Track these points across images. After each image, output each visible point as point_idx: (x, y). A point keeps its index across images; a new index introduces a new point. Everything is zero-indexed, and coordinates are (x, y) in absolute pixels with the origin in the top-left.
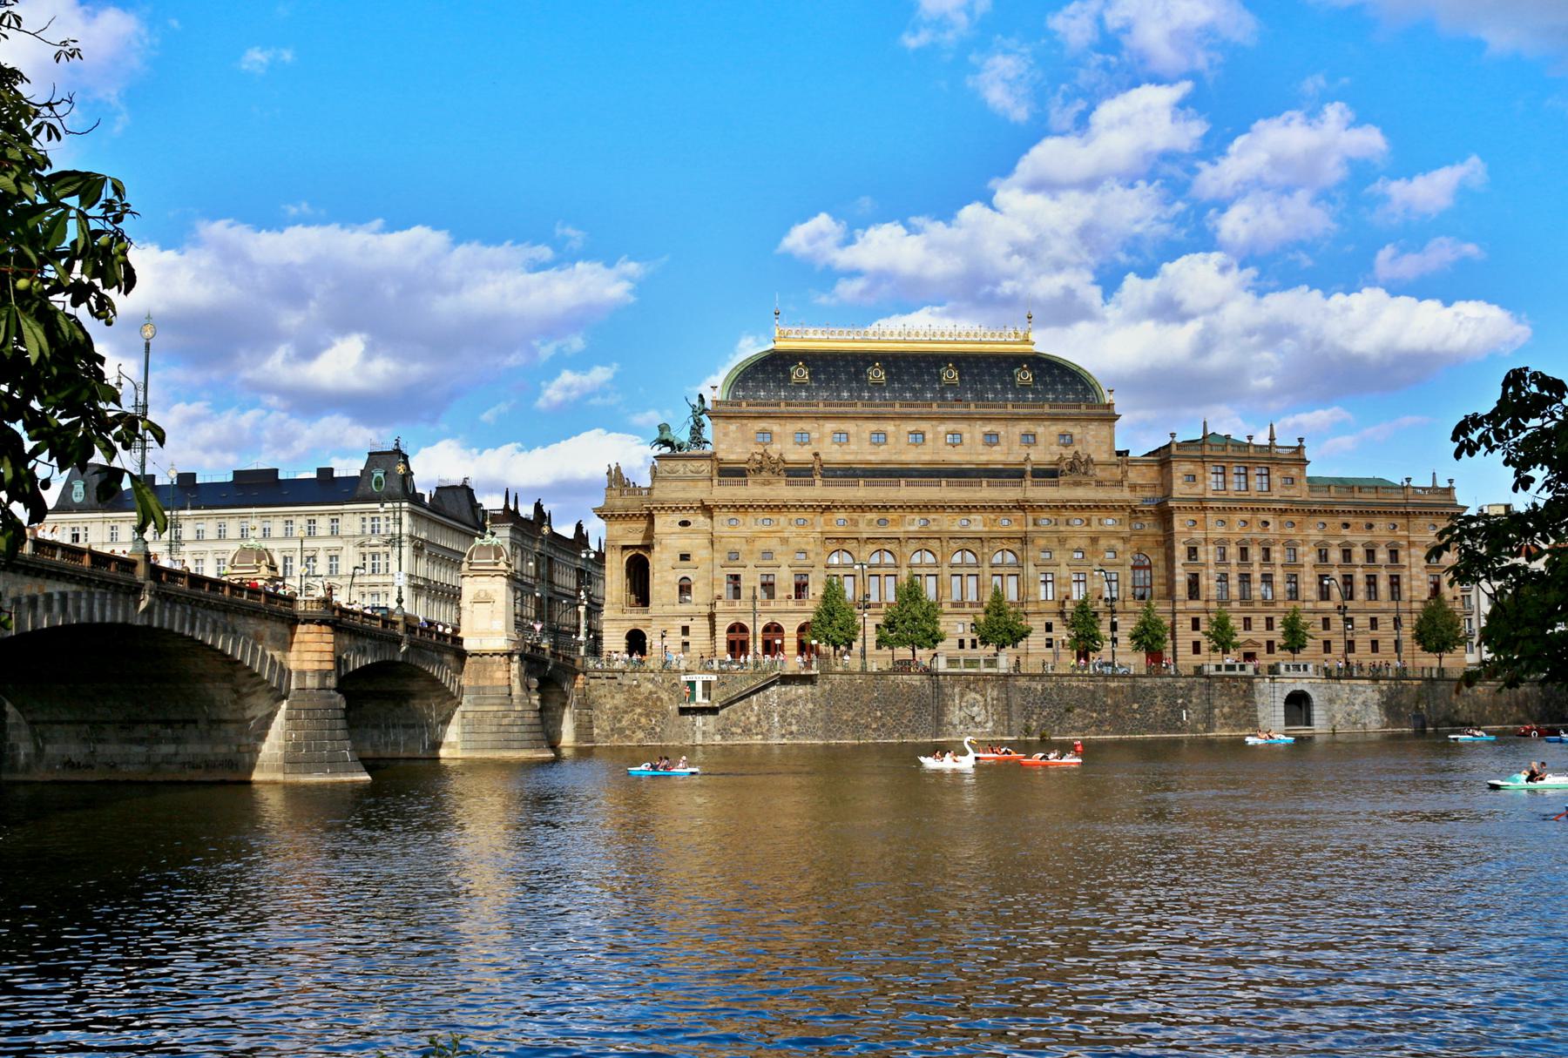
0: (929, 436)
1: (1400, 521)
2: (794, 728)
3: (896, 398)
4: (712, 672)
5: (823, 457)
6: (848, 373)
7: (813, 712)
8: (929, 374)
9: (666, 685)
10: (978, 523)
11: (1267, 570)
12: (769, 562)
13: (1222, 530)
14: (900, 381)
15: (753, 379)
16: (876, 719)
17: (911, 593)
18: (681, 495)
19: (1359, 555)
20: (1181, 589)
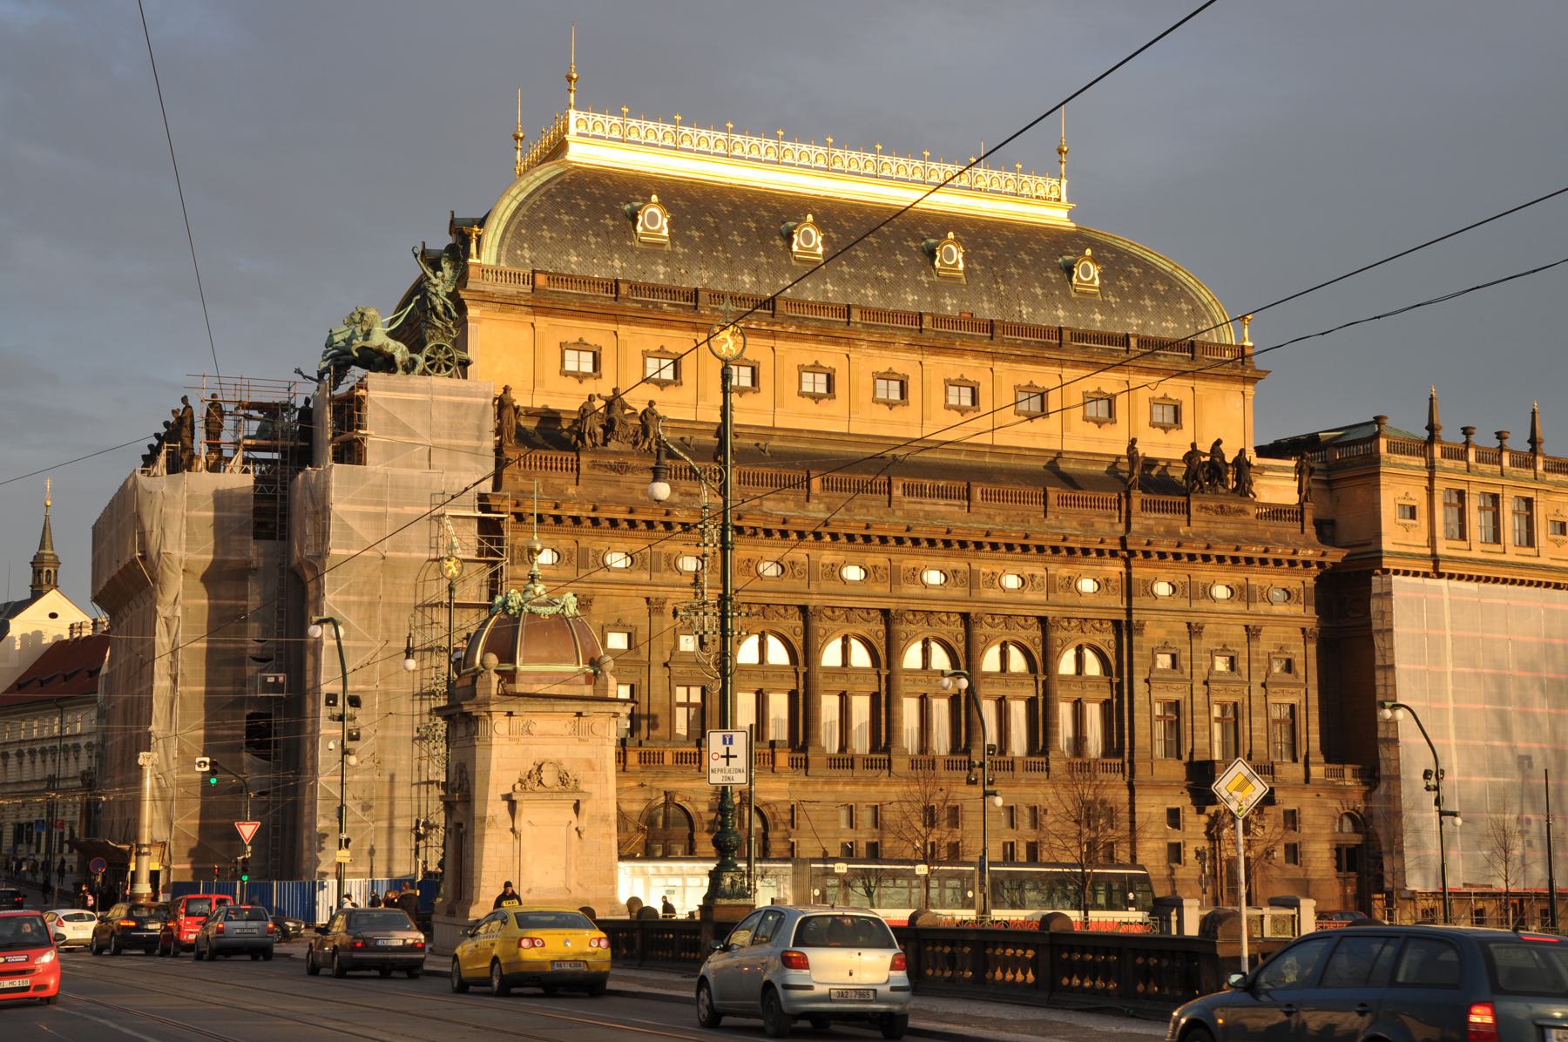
6: (745, 232)
8: (906, 251)
15: (553, 224)
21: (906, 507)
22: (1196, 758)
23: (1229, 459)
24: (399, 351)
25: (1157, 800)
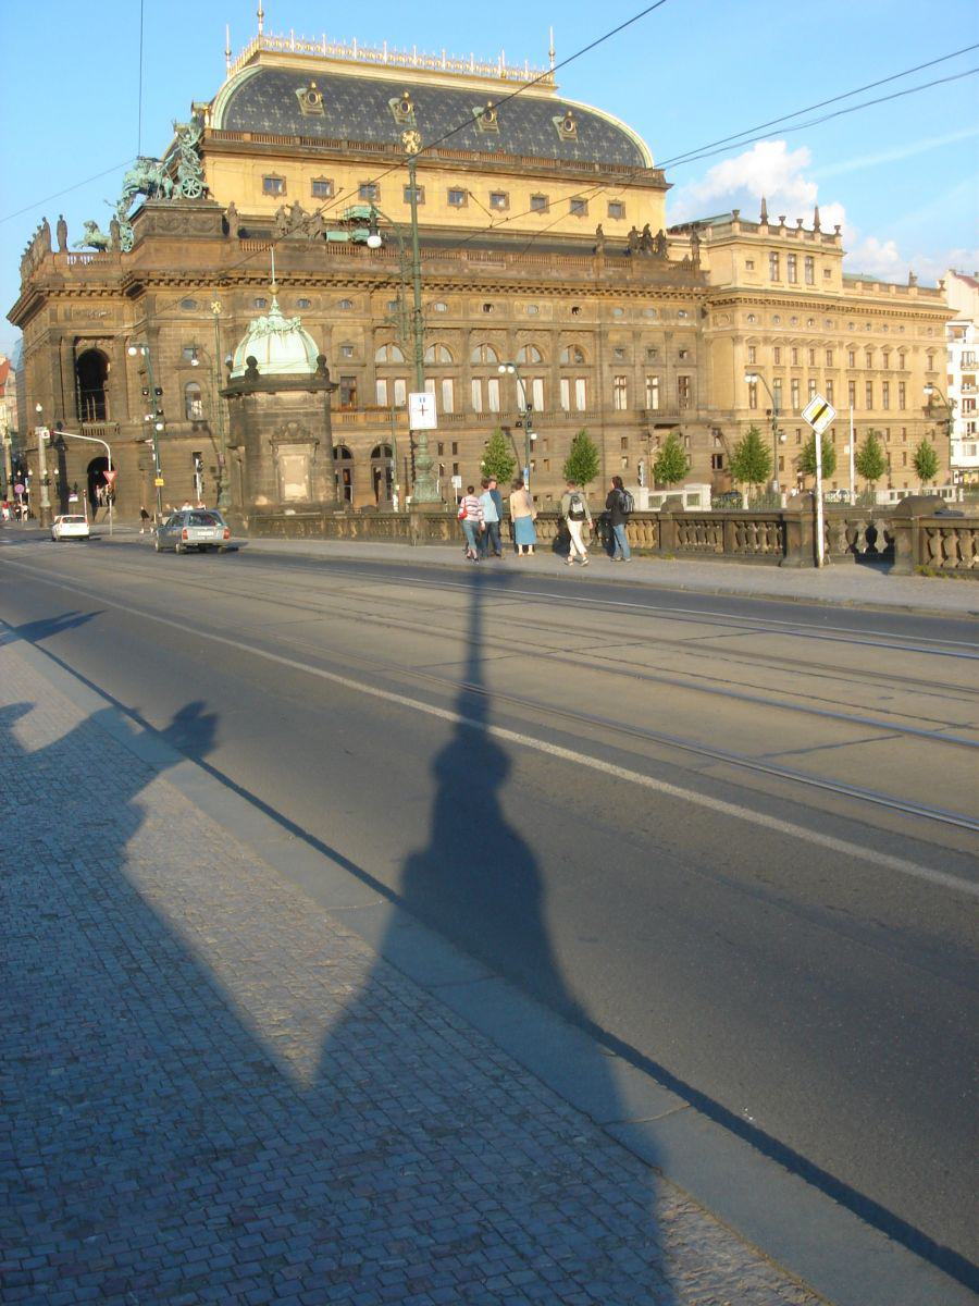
6: (368, 105)
14: (432, 121)
15: (252, 102)
21: (470, 267)
22: (637, 408)
23: (653, 236)
24: (168, 184)
25: (615, 433)
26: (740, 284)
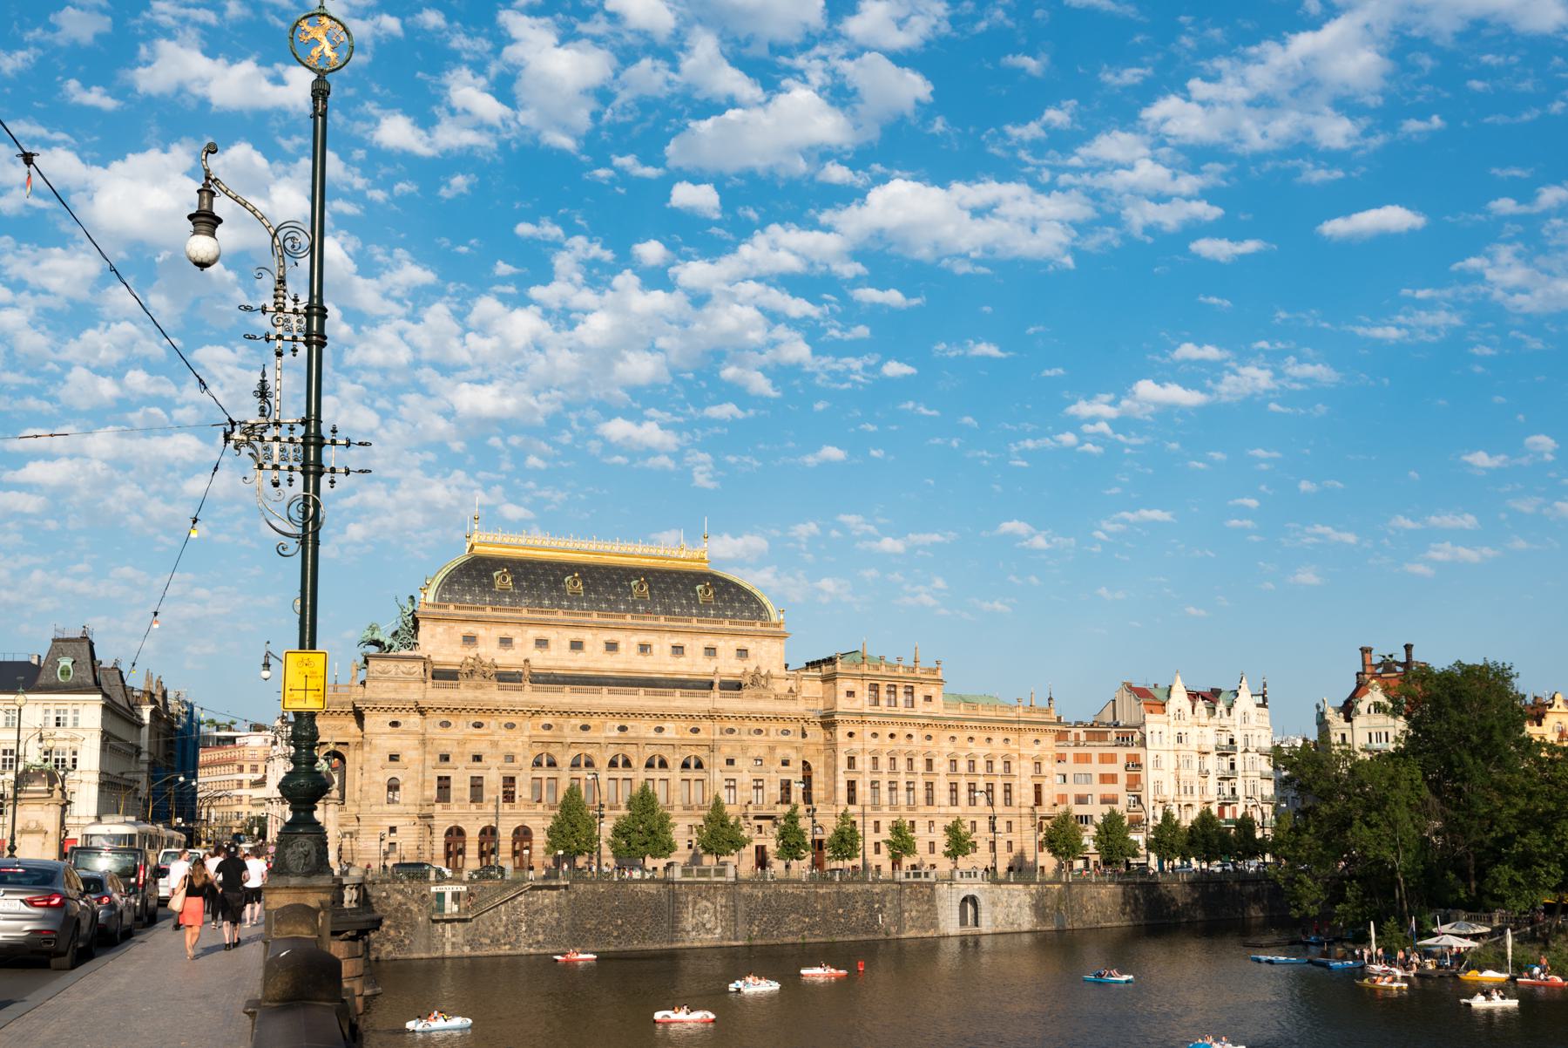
0: (622, 646)
1: (1012, 736)
2: (541, 937)
3: (592, 609)
4: (464, 883)
5: (532, 662)
6: (548, 582)
7: (559, 921)
8: (623, 587)
9: (416, 896)
10: (672, 730)
11: (911, 778)
12: (478, 764)
13: (875, 741)
14: (596, 592)
16: (617, 927)
17: (644, 802)
18: (392, 695)
19: (981, 767)
20: (842, 795)
23: (764, 672)
26: (839, 709)
